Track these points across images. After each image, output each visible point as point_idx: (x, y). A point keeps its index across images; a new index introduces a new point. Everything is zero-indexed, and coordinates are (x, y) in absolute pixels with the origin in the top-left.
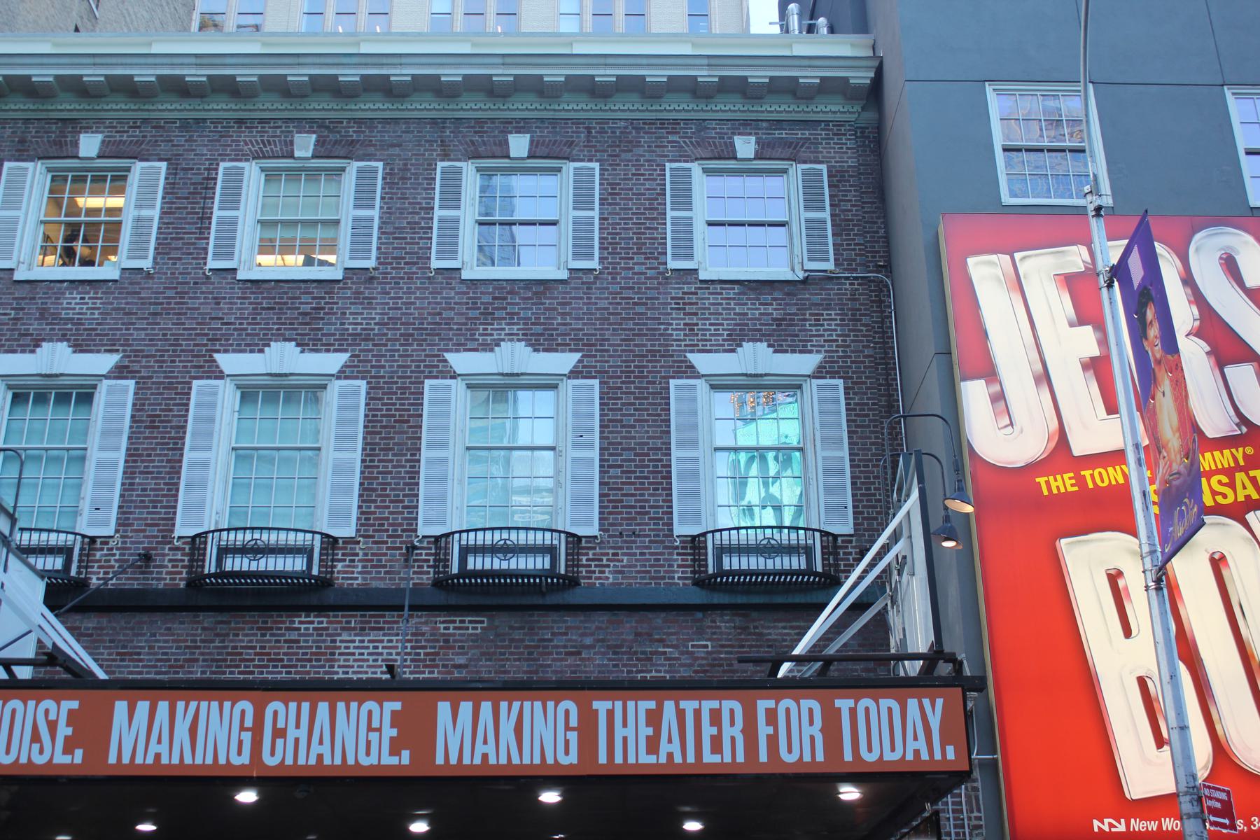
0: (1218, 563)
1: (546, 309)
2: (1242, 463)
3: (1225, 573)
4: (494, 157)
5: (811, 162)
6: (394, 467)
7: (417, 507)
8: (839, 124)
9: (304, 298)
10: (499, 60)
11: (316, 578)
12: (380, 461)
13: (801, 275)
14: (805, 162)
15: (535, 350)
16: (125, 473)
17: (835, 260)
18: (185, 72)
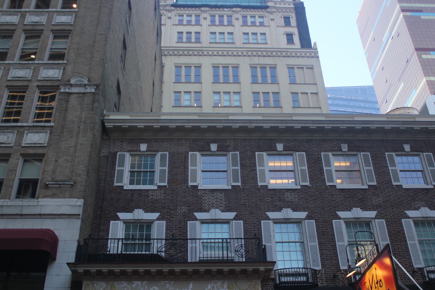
1: (430, 197)
4: (401, 151)
6: (400, 246)
7: (411, 259)
9: (358, 194)
10: (401, 123)
11: (311, 283)
12: (396, 244)
15: (431, 210)
16: (319, 249)
18: (309, 125)
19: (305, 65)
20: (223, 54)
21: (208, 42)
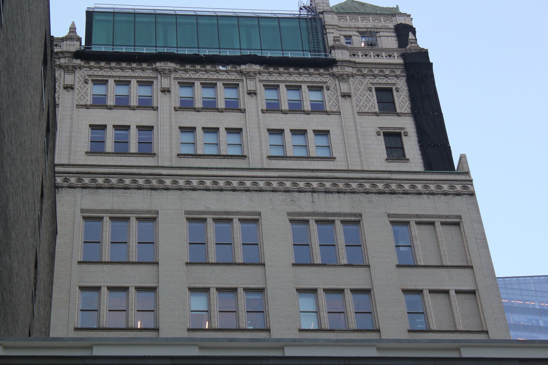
19: (439, 217)
20: (215, 187)
21: (174, 154)
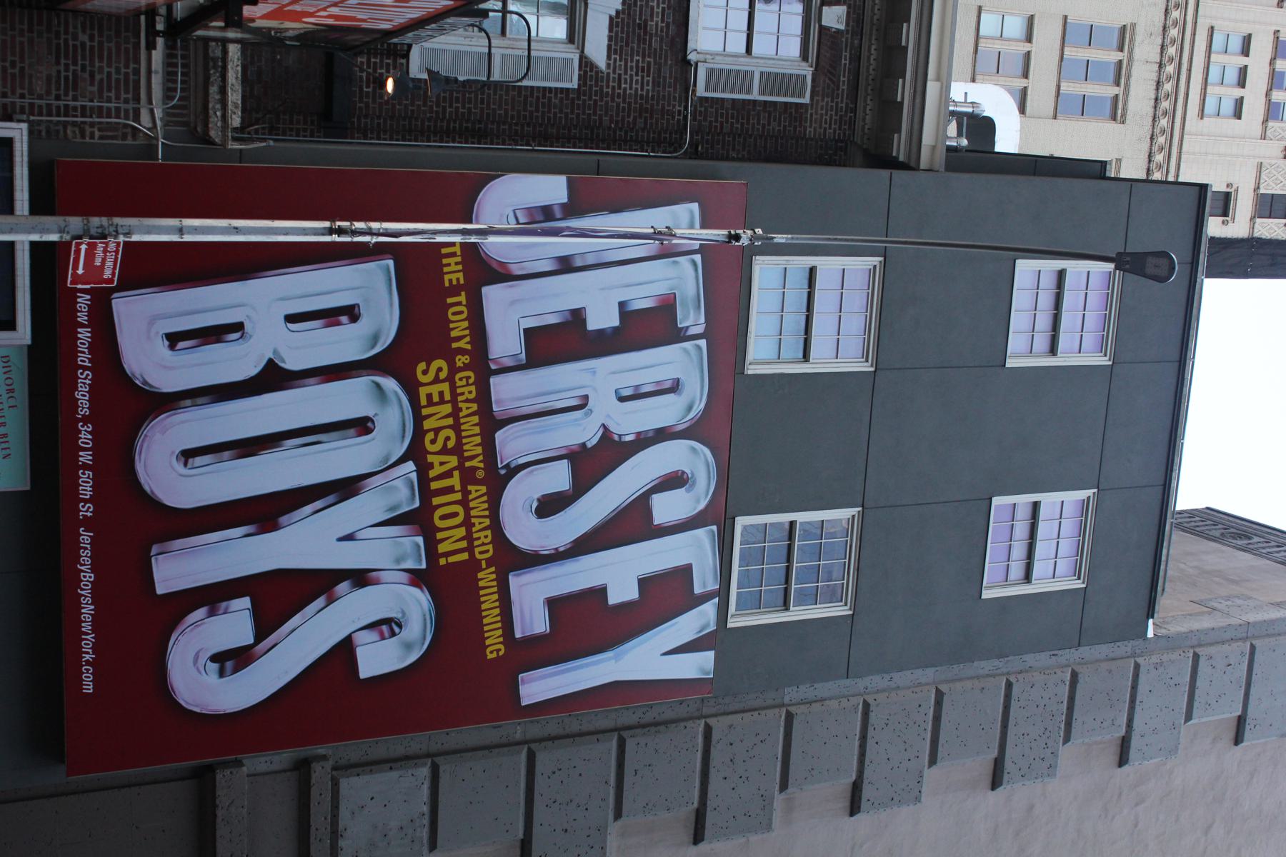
0: (362, 426)
2: (468, 464)
3: (352, 431)
5: (813, 87)
8: (852, 123)
13: (692, 57)
14: (813, 80)
17: (707, 98)
